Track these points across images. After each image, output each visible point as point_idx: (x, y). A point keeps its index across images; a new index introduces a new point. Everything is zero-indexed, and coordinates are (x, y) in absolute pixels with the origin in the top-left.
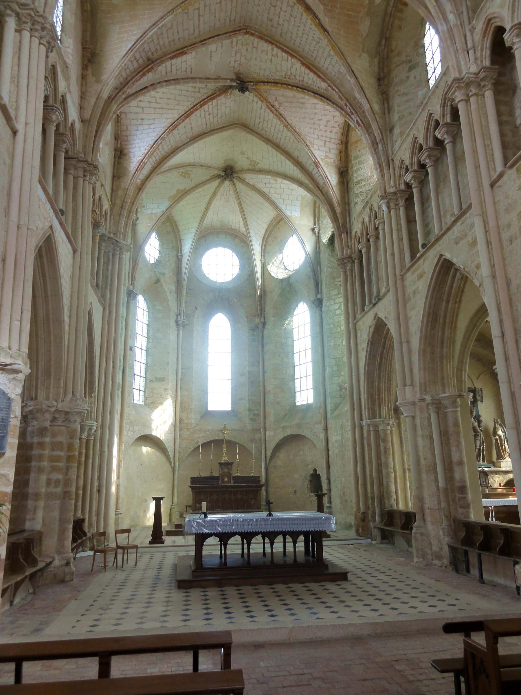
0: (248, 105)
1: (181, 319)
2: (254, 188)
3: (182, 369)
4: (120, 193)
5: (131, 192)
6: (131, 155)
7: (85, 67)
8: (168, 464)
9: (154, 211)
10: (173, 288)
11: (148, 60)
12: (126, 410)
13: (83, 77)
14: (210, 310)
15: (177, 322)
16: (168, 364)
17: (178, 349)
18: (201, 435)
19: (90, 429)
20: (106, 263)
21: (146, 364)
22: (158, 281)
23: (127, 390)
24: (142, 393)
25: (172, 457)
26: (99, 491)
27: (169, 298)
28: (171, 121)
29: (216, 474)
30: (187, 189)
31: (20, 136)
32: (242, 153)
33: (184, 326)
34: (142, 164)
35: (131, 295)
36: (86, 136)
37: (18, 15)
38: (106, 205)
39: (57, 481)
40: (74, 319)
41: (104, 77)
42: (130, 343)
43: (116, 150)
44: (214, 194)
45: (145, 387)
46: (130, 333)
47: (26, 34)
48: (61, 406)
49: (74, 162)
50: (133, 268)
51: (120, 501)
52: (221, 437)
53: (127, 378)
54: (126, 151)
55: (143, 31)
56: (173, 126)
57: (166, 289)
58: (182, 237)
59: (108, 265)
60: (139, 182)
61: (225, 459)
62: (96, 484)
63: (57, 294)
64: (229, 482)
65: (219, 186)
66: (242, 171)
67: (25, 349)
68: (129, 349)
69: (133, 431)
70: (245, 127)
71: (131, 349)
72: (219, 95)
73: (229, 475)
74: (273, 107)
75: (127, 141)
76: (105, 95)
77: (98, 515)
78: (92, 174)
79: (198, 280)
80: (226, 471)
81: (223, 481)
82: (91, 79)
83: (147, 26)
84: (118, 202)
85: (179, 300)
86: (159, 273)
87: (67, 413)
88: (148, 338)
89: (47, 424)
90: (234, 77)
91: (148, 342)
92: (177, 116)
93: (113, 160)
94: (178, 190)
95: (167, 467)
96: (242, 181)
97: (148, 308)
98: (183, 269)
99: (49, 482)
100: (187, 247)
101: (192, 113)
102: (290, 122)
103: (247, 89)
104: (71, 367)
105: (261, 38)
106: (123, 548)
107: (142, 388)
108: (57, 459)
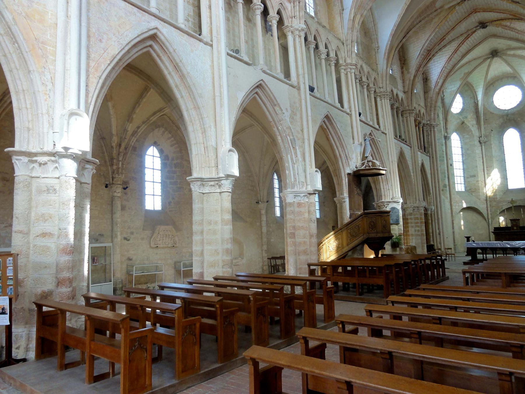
0: (491, 29)
1: (482, 139)
2: (514, 56)
3: (487, 167)
4: (429, 100)
5: (434, 98)
6: (431, 79)
7: (402, 68)
8: (484, 221)
9: (453, 89)
10: (475, 122)
11: (428, 51)
12: (453, 196)
13: (402, 73)
14: (502, 129)
15: (480, 141)
16: (477, 167)
17: (482, 157)
18: (504, 204)
19: (432, 209)
20: (428, 136)
21: (464, 169)
22: (463, 123)
23: (451, 186)
24: (463, 185)
25: (486, 216)
26: (439, 234)
27: (472, 130)
28: (448, 56)
29: (509, 225)
30: (470, 71)
31: (388, 134)
32: (499, 43)
33: (485, 143)
34: (437, 83)
35: (447, 138)
36: (407, 98)
37: (380, 96)
38: (423, 111)
39: (418, 231)
40: (415, 173)
41: (410, 70)
42: (450, 162)
43: (423, 79)
44: (489, 66)
45: (465, 181)
46: (449, 157)
47: (383, 100)
48: (415, 205)
49: (404, 112)
50: (446, 123)
51: (455, 239)
52: (511, 206)
53: (451, 181)
54: (429, 78)
55: (423, 44)
56: (450, 59)
57: (469, 125)
58: (476, 90)
59: (428, 136)
60: (437, 90)
61: (515, 217)
62: (438, 231)
63: (407, 167)
64: (517, 229)
65: (490, 62)
66: (503, 50)
67: (400, 196)
68: (450, 165)
69: (459, 206)
70: (494, 36)
71: (451, 165)
72: (472, 35)
73: (517, 226)
74: (506, 26)
75: (428, 72)
76: (412, 78)
77: (440, 243)
78: (412, 113)
79: (491, 113)
80: (514, 223)
81: (513, 229)
82: (405, 72)
83: (424, 42)
84: (429, 104)
85: (479, 128)
86: (463, 118)
87: (418, 207)
88: (462, 155)
89: (412, 211)
90: (477, 24)
91: (463, 157)
92: (451, 53)
93: (423, 85)
94: (464, 74)
95: (484, 223)
96: (506, 55)
97: (460, 138)
98: (480, 110)
99: (415, 231)
100: (480, 96)
101: (458, 49)
102: (519, 29)
103: (487, 26)
104: (417, 190)
105: (484, 11)
106: (449, 254)
107: (463, 182)
108: (417, 223)
